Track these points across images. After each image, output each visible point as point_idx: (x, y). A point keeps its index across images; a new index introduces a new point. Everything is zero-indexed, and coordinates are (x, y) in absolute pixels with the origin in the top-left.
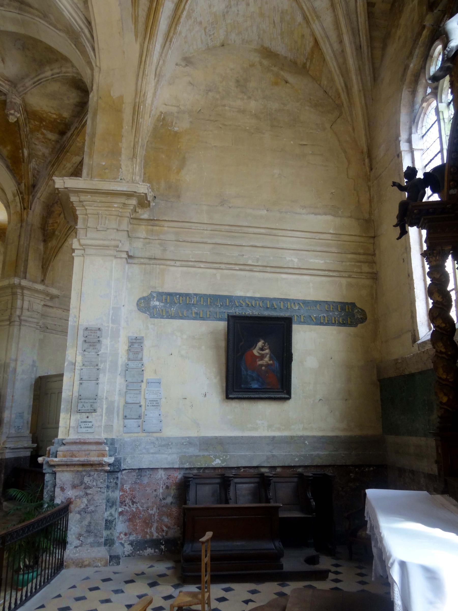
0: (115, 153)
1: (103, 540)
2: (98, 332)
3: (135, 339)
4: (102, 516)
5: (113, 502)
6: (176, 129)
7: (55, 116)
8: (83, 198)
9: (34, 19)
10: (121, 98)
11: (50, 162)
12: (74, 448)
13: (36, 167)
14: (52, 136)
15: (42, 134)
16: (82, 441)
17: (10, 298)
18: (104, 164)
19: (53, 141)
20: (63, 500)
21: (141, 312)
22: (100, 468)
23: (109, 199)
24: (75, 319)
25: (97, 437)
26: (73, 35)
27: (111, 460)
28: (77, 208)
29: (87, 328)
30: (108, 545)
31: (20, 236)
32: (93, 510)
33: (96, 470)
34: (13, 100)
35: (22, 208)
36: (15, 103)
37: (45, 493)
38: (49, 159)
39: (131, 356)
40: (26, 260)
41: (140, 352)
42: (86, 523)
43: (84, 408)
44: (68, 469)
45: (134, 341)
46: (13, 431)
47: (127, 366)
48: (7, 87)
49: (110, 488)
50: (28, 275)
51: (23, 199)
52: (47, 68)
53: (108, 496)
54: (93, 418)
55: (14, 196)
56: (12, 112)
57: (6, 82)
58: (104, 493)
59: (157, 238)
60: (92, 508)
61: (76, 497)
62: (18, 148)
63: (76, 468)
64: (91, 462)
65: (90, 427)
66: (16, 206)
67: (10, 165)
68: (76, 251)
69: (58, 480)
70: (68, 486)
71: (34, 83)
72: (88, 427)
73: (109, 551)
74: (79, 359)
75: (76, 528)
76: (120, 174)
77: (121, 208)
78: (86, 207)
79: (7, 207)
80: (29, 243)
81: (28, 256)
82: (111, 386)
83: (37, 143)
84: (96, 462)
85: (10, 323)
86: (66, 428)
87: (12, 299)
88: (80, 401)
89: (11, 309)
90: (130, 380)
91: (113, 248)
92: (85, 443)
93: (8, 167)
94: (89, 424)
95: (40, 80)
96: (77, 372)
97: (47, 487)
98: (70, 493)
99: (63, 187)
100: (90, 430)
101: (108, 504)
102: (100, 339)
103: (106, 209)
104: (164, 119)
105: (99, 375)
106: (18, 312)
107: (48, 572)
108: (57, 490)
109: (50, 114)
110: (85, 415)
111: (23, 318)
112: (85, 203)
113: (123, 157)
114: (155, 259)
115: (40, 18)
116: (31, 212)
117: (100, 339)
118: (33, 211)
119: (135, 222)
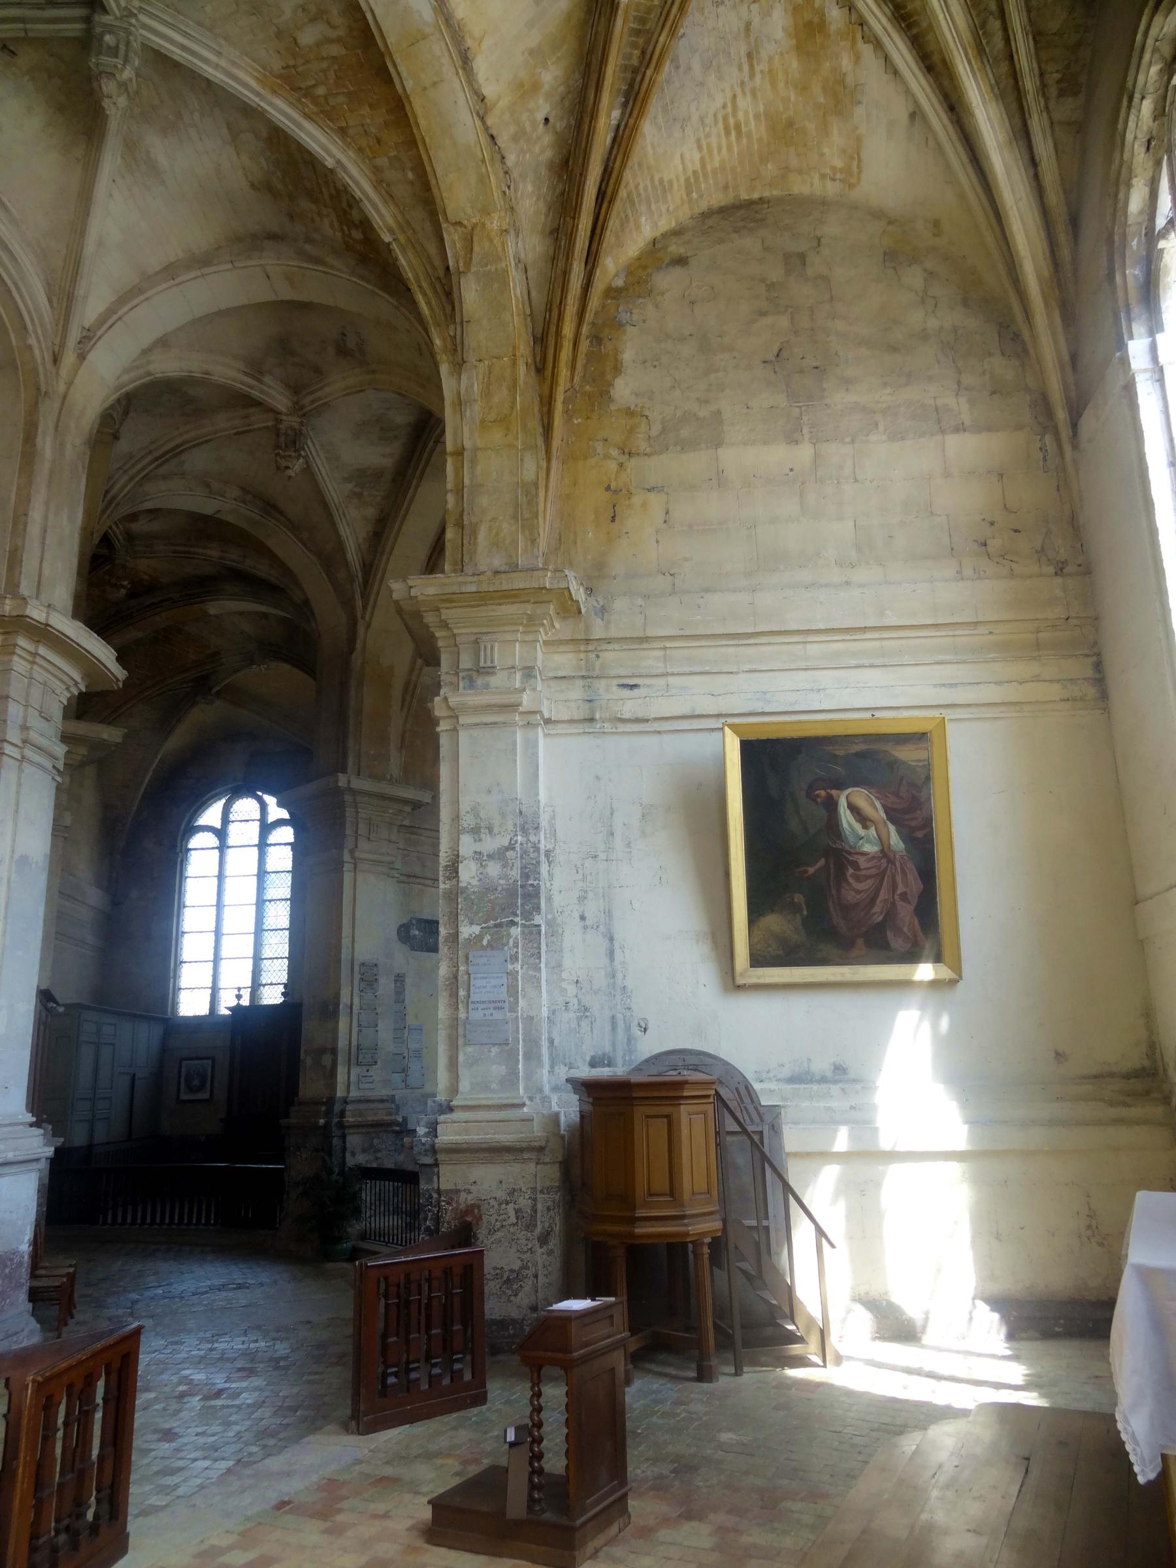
7: (146, 577)
12: (363, 1106)
33: (386, 1131)
54: (376, 1073)
69: (348, 1145)
82: (385, 1034)
92: (368, 1101)
95: (188, 552)
108: (348, 1155)
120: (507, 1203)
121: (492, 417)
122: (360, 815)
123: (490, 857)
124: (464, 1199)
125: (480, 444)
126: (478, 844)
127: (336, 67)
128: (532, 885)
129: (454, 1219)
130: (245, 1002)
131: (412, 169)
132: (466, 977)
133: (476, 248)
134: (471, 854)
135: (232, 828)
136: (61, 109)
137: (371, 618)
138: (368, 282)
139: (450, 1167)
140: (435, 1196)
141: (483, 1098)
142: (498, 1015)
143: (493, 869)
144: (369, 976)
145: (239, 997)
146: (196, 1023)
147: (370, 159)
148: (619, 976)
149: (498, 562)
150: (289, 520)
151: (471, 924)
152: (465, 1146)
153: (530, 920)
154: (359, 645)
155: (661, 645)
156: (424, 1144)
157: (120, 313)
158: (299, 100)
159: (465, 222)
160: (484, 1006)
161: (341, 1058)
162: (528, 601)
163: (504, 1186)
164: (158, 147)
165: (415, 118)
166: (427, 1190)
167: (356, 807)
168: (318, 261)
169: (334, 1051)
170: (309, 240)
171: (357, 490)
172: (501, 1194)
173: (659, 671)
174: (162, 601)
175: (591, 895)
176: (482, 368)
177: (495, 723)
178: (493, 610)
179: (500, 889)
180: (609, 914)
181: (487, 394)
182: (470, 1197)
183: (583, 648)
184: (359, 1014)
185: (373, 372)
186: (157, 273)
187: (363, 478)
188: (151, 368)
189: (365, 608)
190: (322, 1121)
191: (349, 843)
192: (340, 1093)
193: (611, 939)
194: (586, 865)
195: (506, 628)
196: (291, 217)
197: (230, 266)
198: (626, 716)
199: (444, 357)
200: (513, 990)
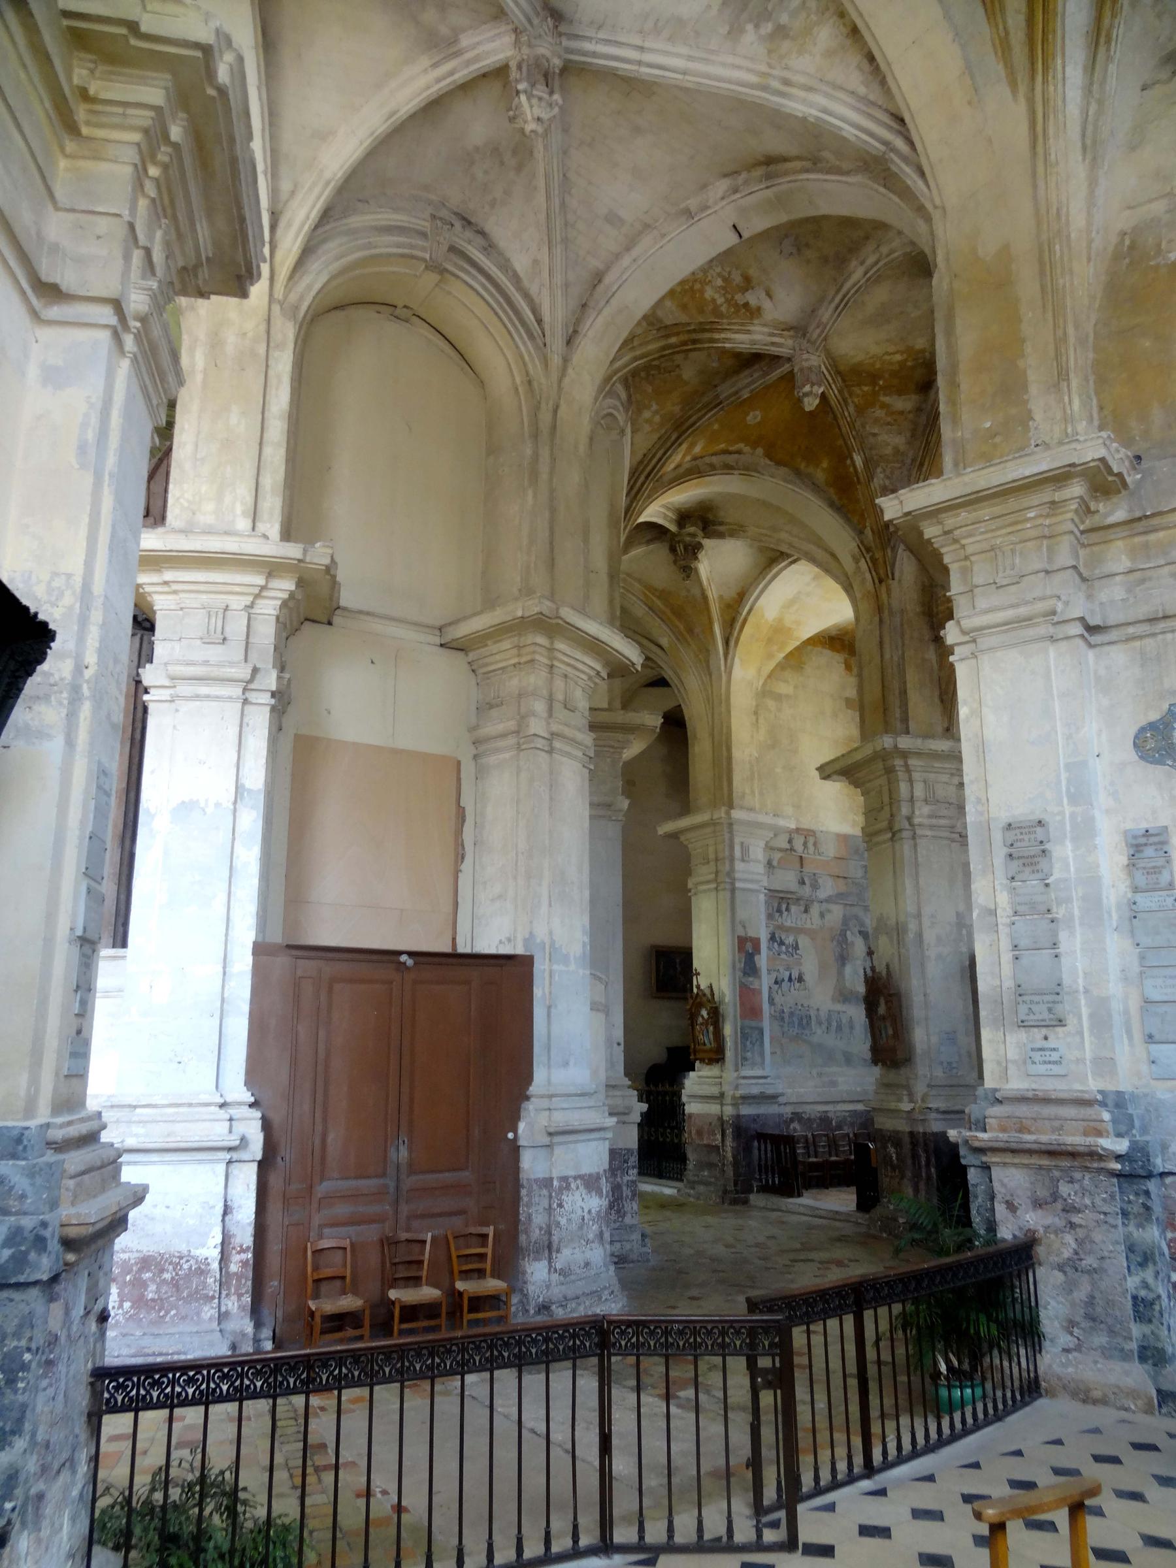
0: (1012, 389)
1: (1134, 1346)
2: (1039, 829)
3: (1144, 836)
4: (1121, 1285)
5: (1145, 1254)
7: (898, 357)
8: (950, 521)
9: (795, 181)
11: (913, 460)
12: (1023, 1110)
13: (887, 482)
14: (904, 403)
15: (884, 406)
16: (1040, 1094)
17: (883, 781)
18: (988, 425)
19: (910, 412)
20: (1017, 1233)
21: (1151, 763)
22: (1095, 1165)
23: (1012, 503)
24: (980, 808)
25: (1077, 1086)
26: (876, 167)
27: (1121, 1146)
28: (943, 550)
29: (1010, 825)
30: (1150, 1362)
31: (881, 643)
32: (1095, 1265)
34: (805, 364)
35: (877, 581)
36: (810, 368)
37: (974, 1212)
38: (911, 454)
39: (1141, 880)
40: (904, 693)
41: (1163, 867)
42: (1081, 1294)
43: (1032, 1017)
44: (1016, 1161)
45: (1143, 840)
46: (939, 1073)
47: (1134, 907)
48: (790, 342)
49: (1131, 1217)
50: (912, 725)
51: (874, 561)
52: (854, 263)
53: (1128, 1236)
54: (1059, 1038)
55: (857, 561)
56: (807, 388)
57: (785, 333)
58: (1115, 1227)
59: (1163, 562)
60: (1089, 1261)
61: (1047, 1228)
62: (842, 456)
63: (1035, 1160)
64: (1070, 1148)
65: (1055, 1063)
66: (864, 580)
67: (835, 498)
68: (957, 650)
69: (996, 1184)
70: (1023, 1201)
71: (837, 308)
72: (1050, 1062)
73: (1154, 1379)
74: (1003, 900)
75: (1058, 1303)
76: (1031, 434)
77: (1048, 516)
78: (963, 542)
79: (848, 588)
80: (903, 654)
81: (905, 683)
83: (876, 431)
84: (1081, 1149)
85: (894, 835)
86: (999, 1063)
87: (889, 783)
88: (1020, 999)
89: (891, 804)
90: (1146, 941)
91: (1042, 619)
92: (1046, 1101)
93: (832, 505)
94: (1054, 1054)
95: (844, 296)
96: (1003, 931)
97: (976, 1197)
98: (1032, 1219)
99: (900, 514)
100: (1056, 1069)
101: (1131, 1256)
102: (1047, 846)
103: (1009, 530)
104: (1132, 247)
105: (1056, 935)
106: (905, 810)
107: (1004, 1396)
108: (1000, 1209)
109: (887, 357)
110: (1038, 1034)
111: (916, 821)
112: (957, 533)
113: (1034, 390)
114: (1165, 617)
115: (807, 171)
116: (894, 584)
117: (1047, 846)
118: (900, 581)
119: (1095, 537)
122: (970, 550)
150: (798, 158)
171: (768, 28)
188: (328, 175)
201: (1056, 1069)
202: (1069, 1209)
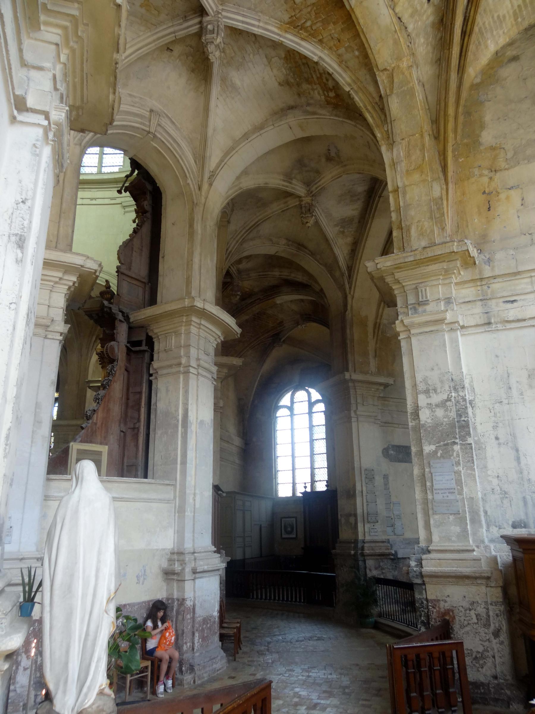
6: (388, 335)
7: (248, 290)
10: (366, 317)
12: (373, 545)
33: (386, 558)
54: (378, 526)
63: (376, 557)
69: (367, 565)
82: (381, 507)
95: (266, 275)
96: (364, 497)
100: (376, 534)
108: (368, 571)
110: (372, 524)
120: (470, 610)
121: (413, 167)
123: (437, 406)
124: (443, 606)
125: (407, 183)
126: (429, 399)
127: (315, 8)
128: (464, 421)
129: (438, 617)
130: (309, 490)
131: (357, 50)
132: (430, 475)
133: (396, 80)
134: (425, 405)
135: (296, 406)
136: (193, 71)
137: (354, 294)
138: (339, 117)
139: (432, 586)
140: (425, 602)
141: (447, 545)
142: (451, 497)
143: (440, 413)
144: (370, 476)
145: (305, 487)
146: (286, 500)
147: (335, 51)
148: (525, 473)
149: (424, 243)
150: (310, 251)
151: (430, 444)
152: (440, 574)
153: (465, 441)
154: (349, 307)
155: (529, 275)
156: (415, 572)
157: (225, 161)
158: (298, 32)
159: (388, 68)
160: (443, 491)
161: (359, 519)
162: (444, 261)
163: (467, 599)
164: (236, 77)
165: (357, 19)
166: (420, 599)
167: (355, 389)
168: (314, 113)
169: (355, 515)
170: (308, 104)
171: (341, 230)
172: (466, 605)
173: (529, 290)
174: (255, 301)
175: (500, 425)
176: (404, 143)
177: (432, 331)
178: (425, 269)
179: (444, 424)
180: (514, 436)
181: (408, 155)
182: (446, 605)
183: (479, 284)
184: (366, 496)
185: (345, 166)
186: (240, 139)
187: (344, 223)
188: (241, 185)
189: (350, 288)
190: (353, 552)
191: (353, 407)
192: (361, 537)
193: (517, 450)
194: (496, 407)
195: (433, 278)
196: (299, 95)
197: (272, 127)
198: (511, 319)
199: (383, 142)
200: (459, 482)
201: (376, 534)
202: (383, 569)
